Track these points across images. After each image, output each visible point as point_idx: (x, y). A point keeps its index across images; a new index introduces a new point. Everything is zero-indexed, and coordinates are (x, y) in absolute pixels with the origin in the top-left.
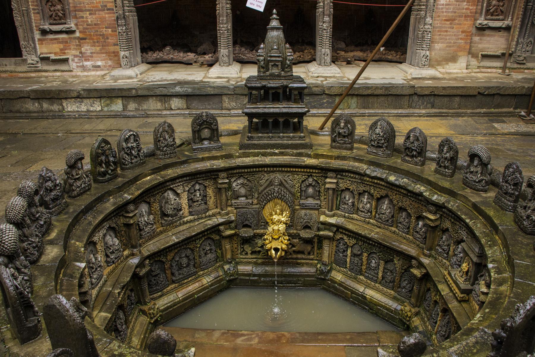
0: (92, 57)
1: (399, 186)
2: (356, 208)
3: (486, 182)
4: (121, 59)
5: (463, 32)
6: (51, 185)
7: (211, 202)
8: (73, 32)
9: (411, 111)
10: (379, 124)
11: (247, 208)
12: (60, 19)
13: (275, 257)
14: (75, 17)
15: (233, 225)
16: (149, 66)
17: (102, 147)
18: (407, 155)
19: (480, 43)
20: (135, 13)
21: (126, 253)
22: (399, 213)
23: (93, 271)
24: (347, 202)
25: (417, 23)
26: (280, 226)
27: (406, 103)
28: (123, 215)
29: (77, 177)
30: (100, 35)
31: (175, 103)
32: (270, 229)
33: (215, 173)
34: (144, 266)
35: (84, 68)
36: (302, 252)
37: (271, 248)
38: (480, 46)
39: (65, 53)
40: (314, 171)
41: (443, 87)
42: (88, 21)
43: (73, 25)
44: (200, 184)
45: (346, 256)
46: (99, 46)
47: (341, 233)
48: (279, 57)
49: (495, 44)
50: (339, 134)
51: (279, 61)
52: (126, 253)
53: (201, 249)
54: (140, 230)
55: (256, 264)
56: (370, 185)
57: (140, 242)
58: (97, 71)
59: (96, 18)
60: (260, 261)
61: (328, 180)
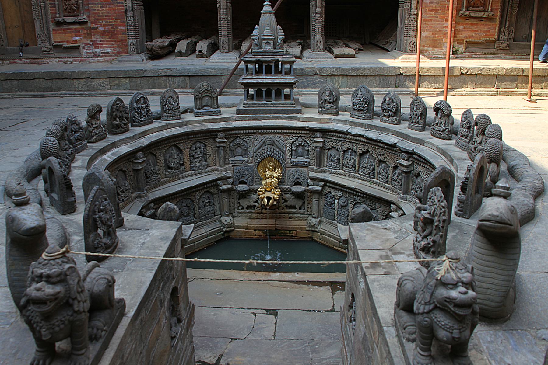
2: (341, 164)
24: (333, 159)
27: (393, 82)
28: (132, 162)
32: (264, 182)
33: (214, 134)
35: (95, 55)
40: (303, 132)
45: (334, 209)
52: (134, 195)
54: (147, 178)
57: (147, 187)
58: (106, 56)
61: (316, 140)
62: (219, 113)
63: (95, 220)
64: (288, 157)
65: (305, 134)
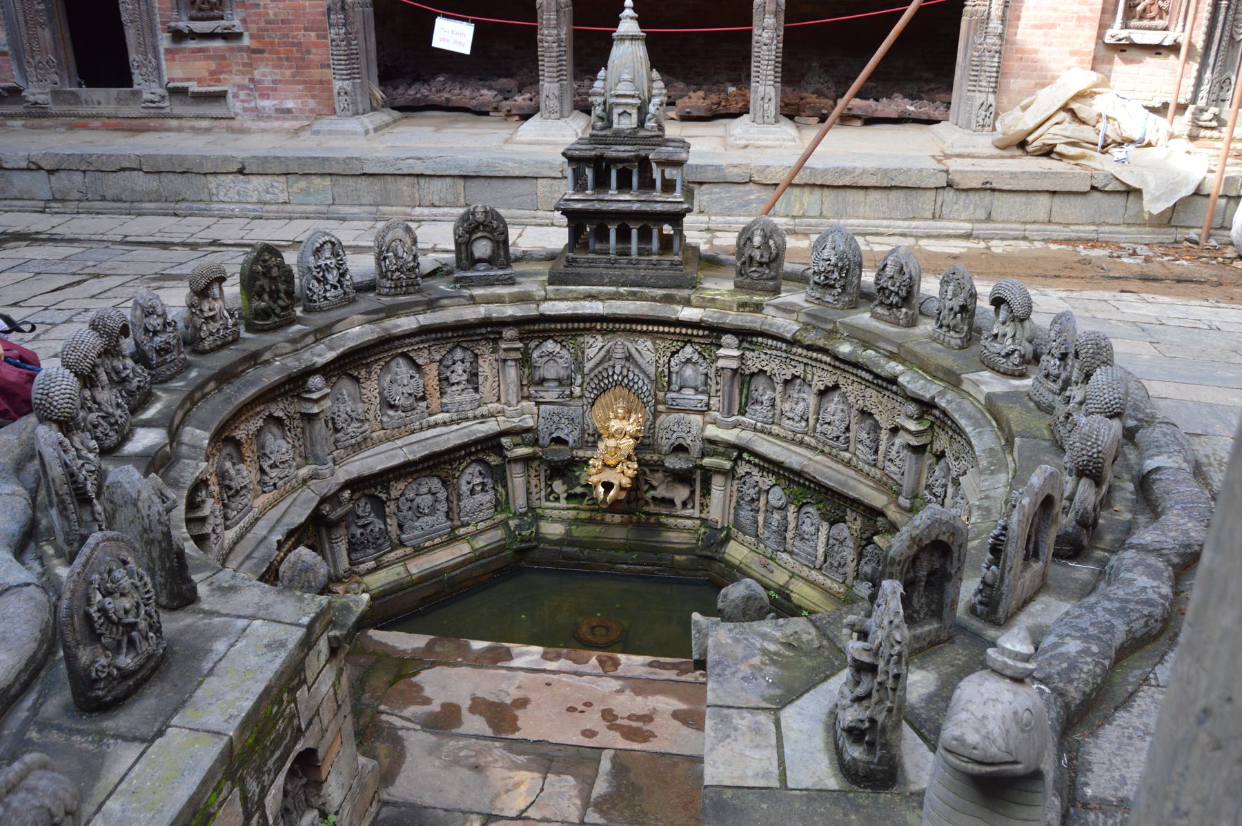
0: (275, 89)
1: (856, 365)
2: (778, 412)
3: (1022, 356)
4: (336, 97)
6: (155, 323)
7: (486, 388)
8: (239, 36)
9: (939, 224)
12: (211, 9)
13: (604, 500)
16: (396, 114)
17: (265, 261)
18: (881, 303)
21: (304, 471)
23: (230, 493)
24: (760, 399)
25: (972, 32)
26: (624, 441)
29: (211, 314)
30: (293, 44)
32: (601, 445)
33: (497, 329)
34: (340, 503)
35: (259, 114)
39: (218, 81)
40: (695, 332)
41: (1011, 173)
42: (267, 14)
43: (236, 22)
44: (465, 349)
46: (289, 68)
47: (749, 462)
48: (633, 97)
50: (751, 258)
51: (633, 105)
52: (304, 471)
53: (463, 482)
54: (337, 431)
56: (806, 364)
58: (285, 119)
59: (284, 9)
61: (722, 352)
62: (510, 281)
65: (703, 337)
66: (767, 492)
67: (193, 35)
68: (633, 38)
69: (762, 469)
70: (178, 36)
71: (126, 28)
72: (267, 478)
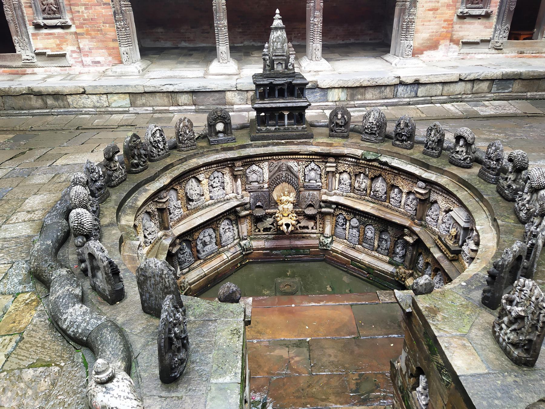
2: (353, 188)
3: (470, 159)
5: (445, 21)
8: (69, 27)
10: (372, 114)
11: (259, 191)
12: (54, 14)
13: (287, 232)
14: (71, 11)
15: (248, 206)
18: (398, 140)
19: (461, 31)
20: (131, 8)
22: (391, 190)
25: (402, 14)
29: (115, 168)
31: (184, 99)
36: (307, 228)
37: (282, 224)
38: (461, 34)
42: (84, 16)
44: (218, 172)
47: (340, 209)
48: (283, 56)
49: (475, 30)
50: (337, 123)
53: (221, 229)
55: (267, 239)
60: (271, 237)
61: (328, 164)
63: (170, 339)
64: (301, 181)
65: (319, 159)
66: (350, 221)
67: (46, 27)
68: (281, 28)
69: (346, 211)
70: (38, 27)
71: (9, 23)
72: (147, 240)
